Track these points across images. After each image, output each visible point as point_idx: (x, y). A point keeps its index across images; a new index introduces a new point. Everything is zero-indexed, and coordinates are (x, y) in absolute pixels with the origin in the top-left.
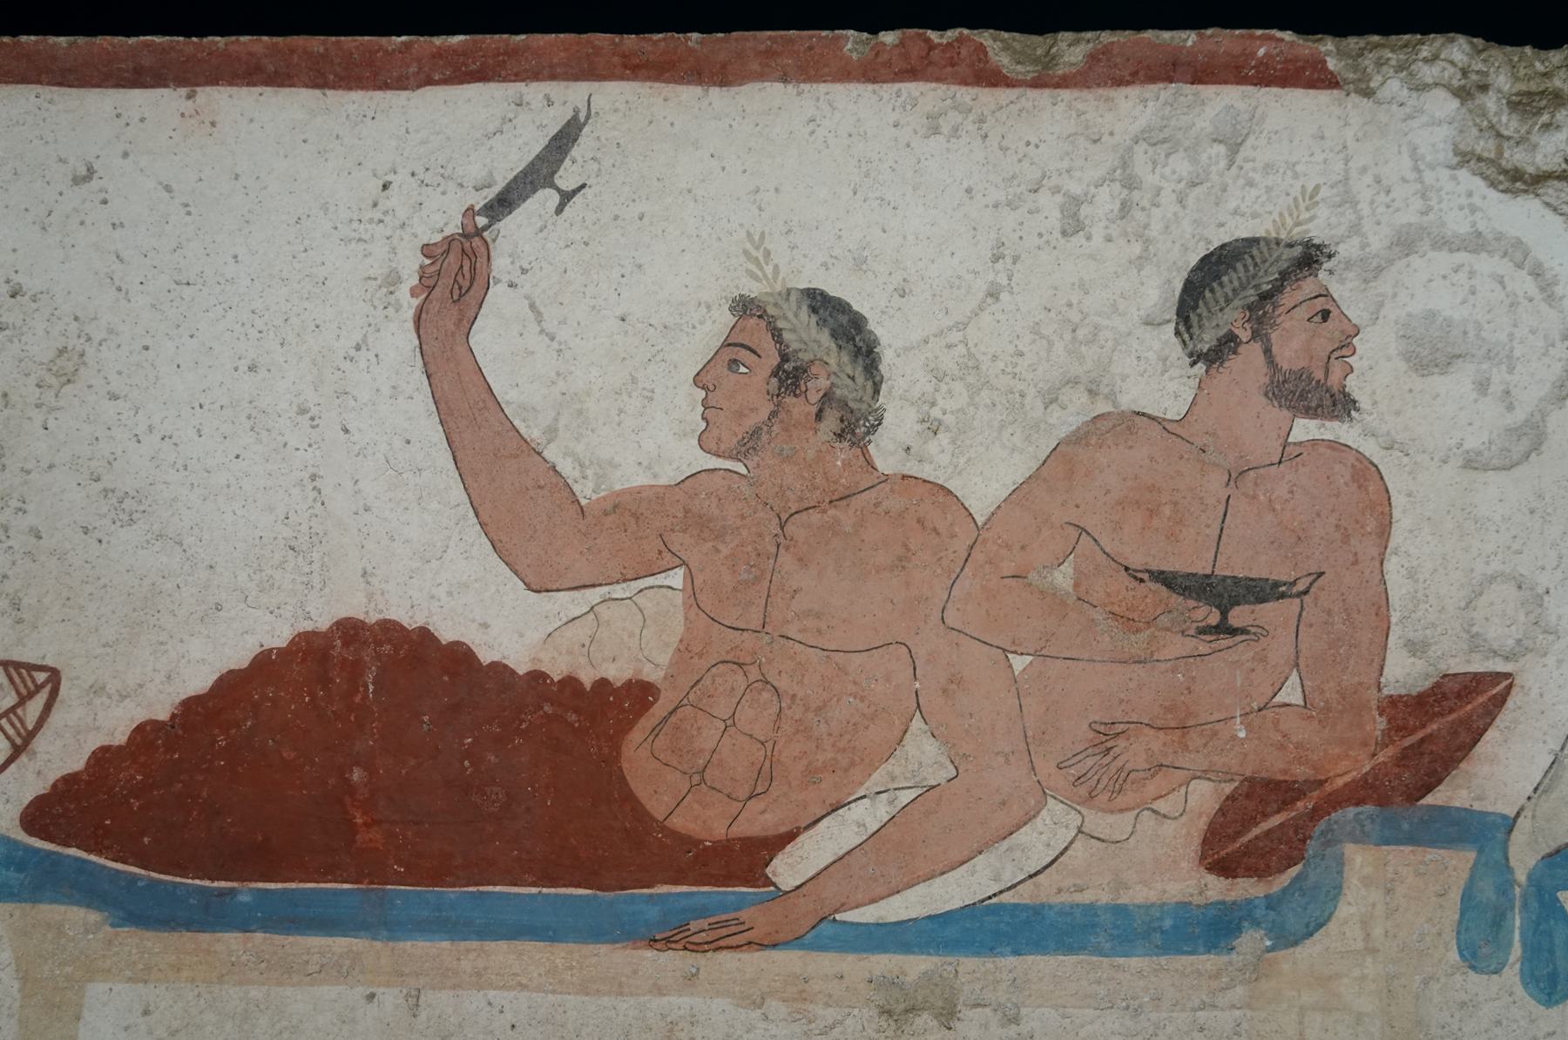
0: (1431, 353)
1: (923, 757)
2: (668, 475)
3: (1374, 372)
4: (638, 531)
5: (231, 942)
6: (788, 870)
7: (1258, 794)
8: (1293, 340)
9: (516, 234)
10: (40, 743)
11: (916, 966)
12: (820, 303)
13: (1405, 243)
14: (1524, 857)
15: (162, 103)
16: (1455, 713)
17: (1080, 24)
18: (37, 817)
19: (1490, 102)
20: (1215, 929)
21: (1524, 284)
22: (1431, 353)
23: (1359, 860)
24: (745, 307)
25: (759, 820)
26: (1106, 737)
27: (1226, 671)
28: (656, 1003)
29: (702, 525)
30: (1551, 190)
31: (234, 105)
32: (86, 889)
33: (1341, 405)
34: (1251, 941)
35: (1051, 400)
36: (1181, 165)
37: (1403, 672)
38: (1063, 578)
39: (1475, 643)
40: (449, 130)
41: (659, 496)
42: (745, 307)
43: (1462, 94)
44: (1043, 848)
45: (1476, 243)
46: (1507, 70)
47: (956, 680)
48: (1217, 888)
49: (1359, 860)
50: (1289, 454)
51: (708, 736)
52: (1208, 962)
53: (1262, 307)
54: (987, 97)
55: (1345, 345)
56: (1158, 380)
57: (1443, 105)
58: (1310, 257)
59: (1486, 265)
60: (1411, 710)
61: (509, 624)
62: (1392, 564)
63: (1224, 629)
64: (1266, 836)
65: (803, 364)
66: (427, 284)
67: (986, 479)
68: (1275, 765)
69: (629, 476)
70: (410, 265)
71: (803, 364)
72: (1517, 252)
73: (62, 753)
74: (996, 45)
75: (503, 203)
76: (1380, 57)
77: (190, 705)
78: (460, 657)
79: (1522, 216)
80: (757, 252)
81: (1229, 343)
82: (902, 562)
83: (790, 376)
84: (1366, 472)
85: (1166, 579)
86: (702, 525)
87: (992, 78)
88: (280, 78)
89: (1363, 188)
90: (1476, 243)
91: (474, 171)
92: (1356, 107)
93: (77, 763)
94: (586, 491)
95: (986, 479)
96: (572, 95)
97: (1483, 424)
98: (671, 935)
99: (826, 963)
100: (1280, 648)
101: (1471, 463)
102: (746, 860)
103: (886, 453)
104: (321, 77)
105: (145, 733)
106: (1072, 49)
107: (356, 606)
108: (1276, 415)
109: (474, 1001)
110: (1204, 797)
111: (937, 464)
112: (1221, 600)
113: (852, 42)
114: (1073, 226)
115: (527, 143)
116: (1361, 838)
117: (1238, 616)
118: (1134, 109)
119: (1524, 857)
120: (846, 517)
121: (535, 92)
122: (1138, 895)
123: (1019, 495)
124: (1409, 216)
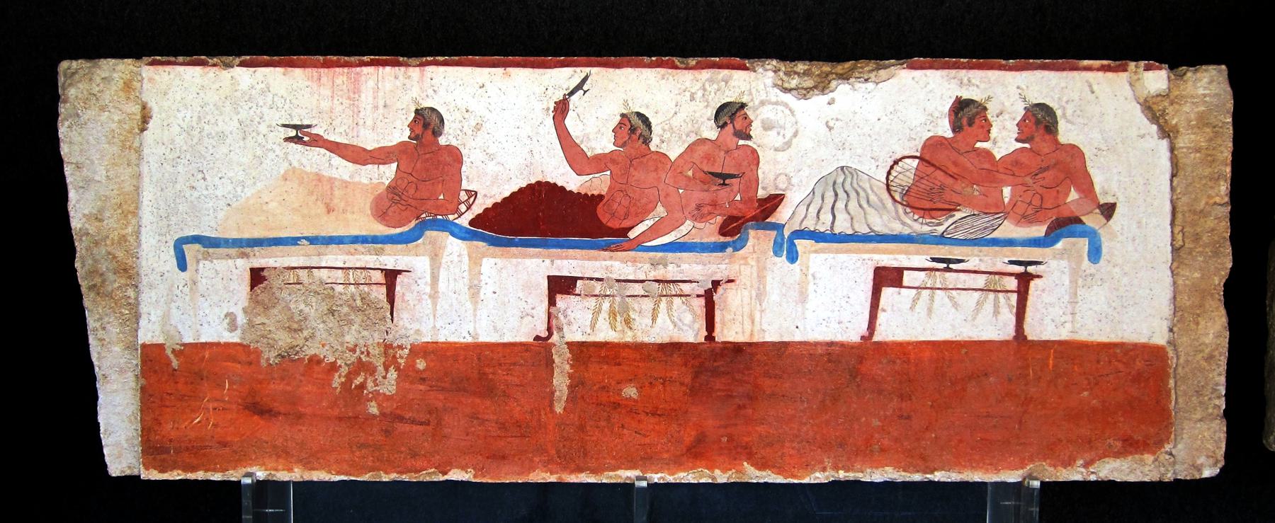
0: (767, 127)
1: (660, 211)
2: (607, 151)
3: (756, 130)
4: (600, 163)
5: (514, 249)
6: (632, 234)
7: (731, 219)
8: (739, 124)
9: (574, 98)
10: (474, 207)
11: (660, 254)
12: (639, 115)
13: (762, 103)
14: (787, 233)
15: (499, 71)
16: (774, 201)
17: (694, 56)
18: (472, 223)
19: (781, 74)
20: (721, 247)
21: (787, 112)
22: (767, 127)
23: (752, 233)
24: (623, 115)
25: (626, 224)
26: (699, 207)
27: (723, 193)
28: (604, 263)
29: (613, 161)
30: (794, 92)
31: (514, 71)
32: (483, 238)
33: (749, 137)
34: (730, 250)
35: (688, 135)
36: (715, 86)
37: (761, 194)
38: (690, 173)
39: (777, 188)
40: (562, 78)
41: (605, 155)
42: (623, 115)
43: (775, 72)
44: (685, 230)
45: (777, 103)
46: (782, 66)
47: (667, 195)
48: (722, 239)
49: (752, 233)
50: (738, 147)
51: (615, 206)
52: (720, 254)
53: (732, 116)
54: (674, 71)
55: (750, 124)
56: (711, 132)
57: (771, 74)
58: (743, 106)
59: (780, 108)
60: (763, 201)
61: (572, 182)
62: (760, 172)
63: (724, 184)
64: (733, 228)
65: (634, 128)
66: (555, 110)
67: (674, 151)
68: (735, 213)
69: (599, 151)
70: (552, 106)
71: (634, 128)
72: (786, 105)
73: (477, 209)
74: (676, 60)
75: (572, 93)
76: (757, 64)
77: (505, 199)
78: (563, 188)
79: (788, 98)
80: (626, 103)
81: (725, 124)
82: (656, 170)
83: (633, 130)
84: (754, 152)
85: (712, 174)
86: (613, 161)
87: (676, 68)
88: (524, 66)
89: (754, 91)
90: (777, 103)
91: (565, 86)
92: (753, 74)
93: (481, 211)
94: (589, 154)
95: (674, 151)
96: (587, 70)
97: (779, 142)
98: (606, 248)
99: (640, 254)
100: (736, 188)
101: (776, 150)
102: (623, 232)
103: (653, 147)
104: (533, 66)
105: (496, 205)
106: (692, 62)
107: (540, 178)
108: (735, 139)
109: (565, 262)
110: (719, 219)
111: (664, 149)
112: (724, 177)
113: (646, 59)
114: (692, 98)
115: (576, 81)
116: (752, 228)
117: (727, 181)
118: (706, 74)
119: (787, 233)
120: (645, 160)
121: (578, 69)
122: (705, 240)
123: (681, 156)
124: (764, 97)
